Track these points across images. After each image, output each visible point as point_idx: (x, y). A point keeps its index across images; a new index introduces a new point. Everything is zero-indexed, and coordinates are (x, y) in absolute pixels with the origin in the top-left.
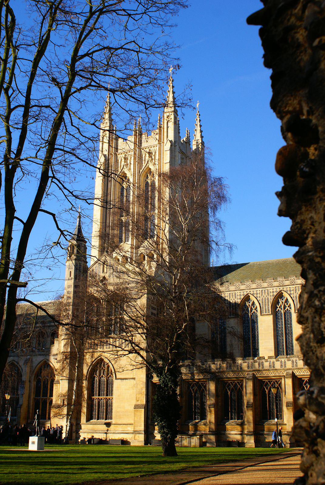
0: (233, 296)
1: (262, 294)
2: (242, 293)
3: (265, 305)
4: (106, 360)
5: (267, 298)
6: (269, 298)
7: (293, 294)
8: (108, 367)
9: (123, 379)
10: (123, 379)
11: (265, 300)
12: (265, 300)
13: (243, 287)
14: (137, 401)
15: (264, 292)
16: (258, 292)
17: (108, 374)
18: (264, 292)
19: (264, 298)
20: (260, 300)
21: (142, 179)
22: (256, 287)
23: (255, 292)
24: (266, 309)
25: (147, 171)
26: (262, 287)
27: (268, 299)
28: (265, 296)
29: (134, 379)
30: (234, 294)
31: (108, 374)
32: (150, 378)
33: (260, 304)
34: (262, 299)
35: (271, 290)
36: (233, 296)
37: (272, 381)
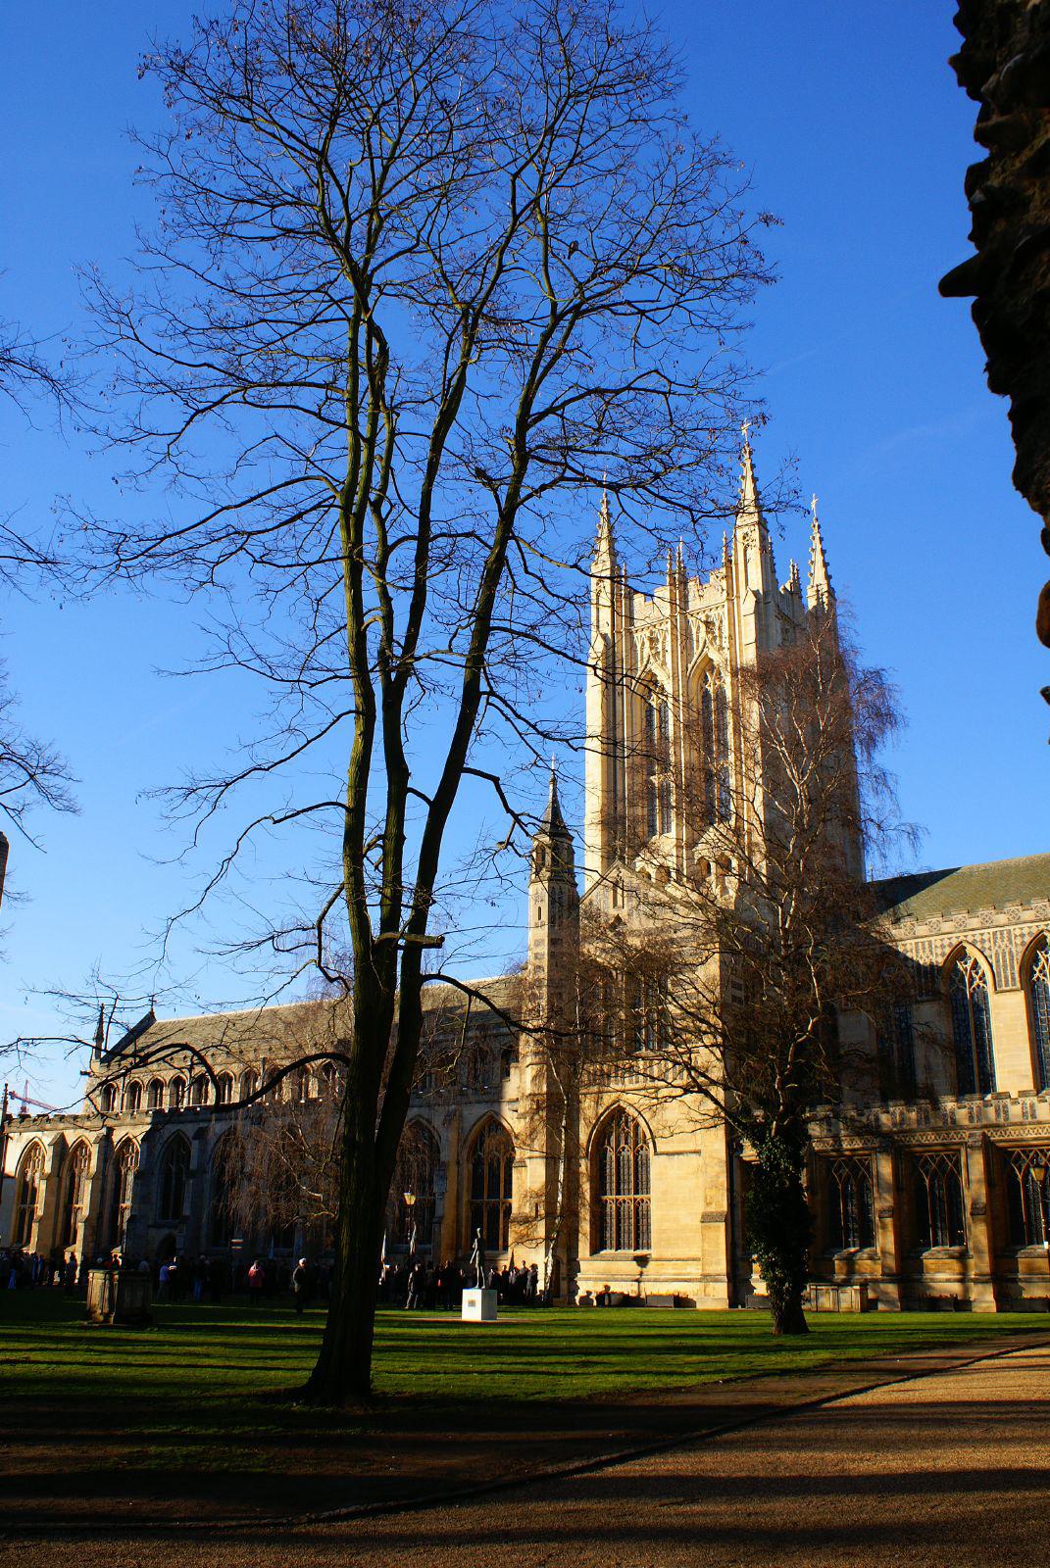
0: (924, 948)
3: (1005, 966)
4: (630, 1111)
5: (1007, 951)
8: (637, 1126)
9: (673, 1154)
10: (673, 1154)
11: (1004, 957)
12: (1004, 957)
13: (947, 927)
14: (708, 1204)
15: (998, 935)
16: (986, 937)
17: (636, 1143)
18: (998, 935)
19: (1000, 951)
21: (694, 685)
22: (979, 925)
23: (978, 938)
24: (1006, 978)
25: (702, 666)
27: (1010, 952)
28: (1003, 947)
29: (698, 1152)
31: (636, 1143)
32: (736, 1150)
33: (991, 965)
34: (997, 954)
35: (1018, 932)
36: (924, 948)
37: (1031, 1151)
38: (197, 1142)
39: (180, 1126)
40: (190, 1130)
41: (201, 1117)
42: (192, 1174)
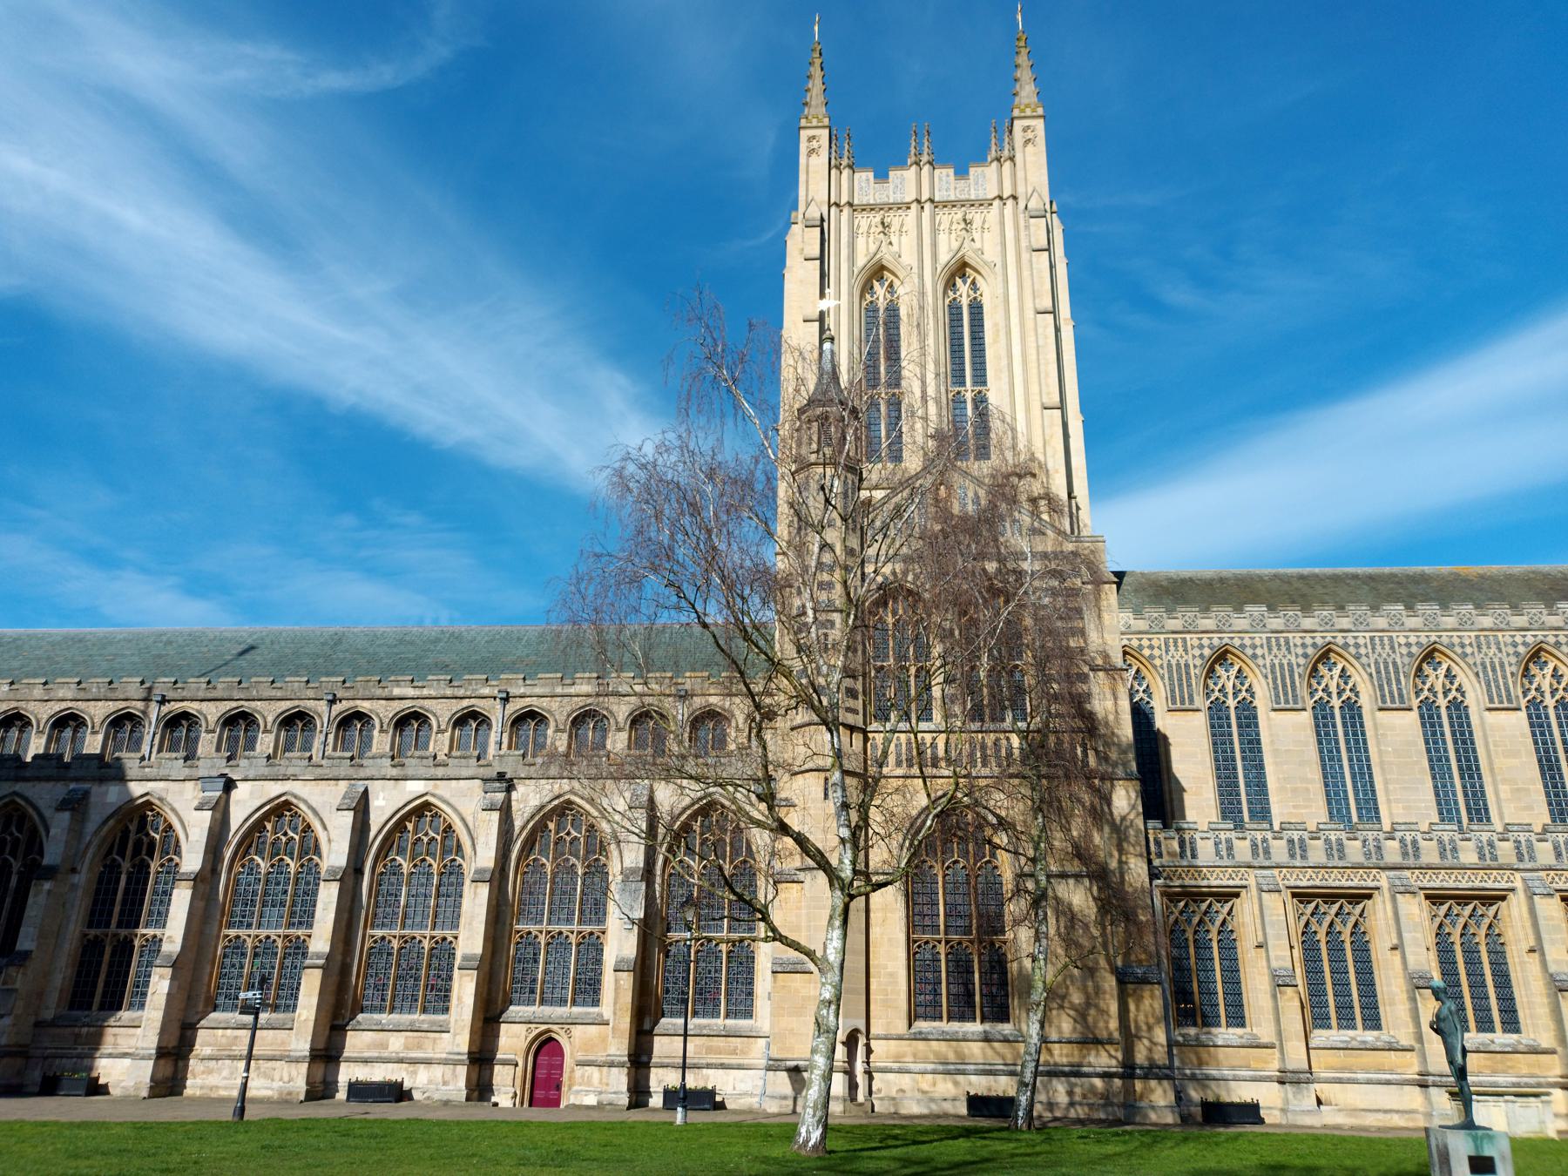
0: (1279, 645)
1: (1373, 649)
2: (1309, 641)
3: (1389, 680)
6: (1398, 660)
7: (1473, 654)
11: (1386, 668)
12: (1386, 668)
13: (1308, 623)
20: (1369, 665)
23: (1351, 641)
24: (1391, 693)
26: (1371, 627)
27: (1395, 663)
28: (1384, 655)
30: (1282, 640)
34: (1376, 662)
35: (1402, 641)
36: (1279, 645)
38: (66, 815)
39: (18, 787)
40: (44, 795)
41: (72, 773)
42: (50, 873)
